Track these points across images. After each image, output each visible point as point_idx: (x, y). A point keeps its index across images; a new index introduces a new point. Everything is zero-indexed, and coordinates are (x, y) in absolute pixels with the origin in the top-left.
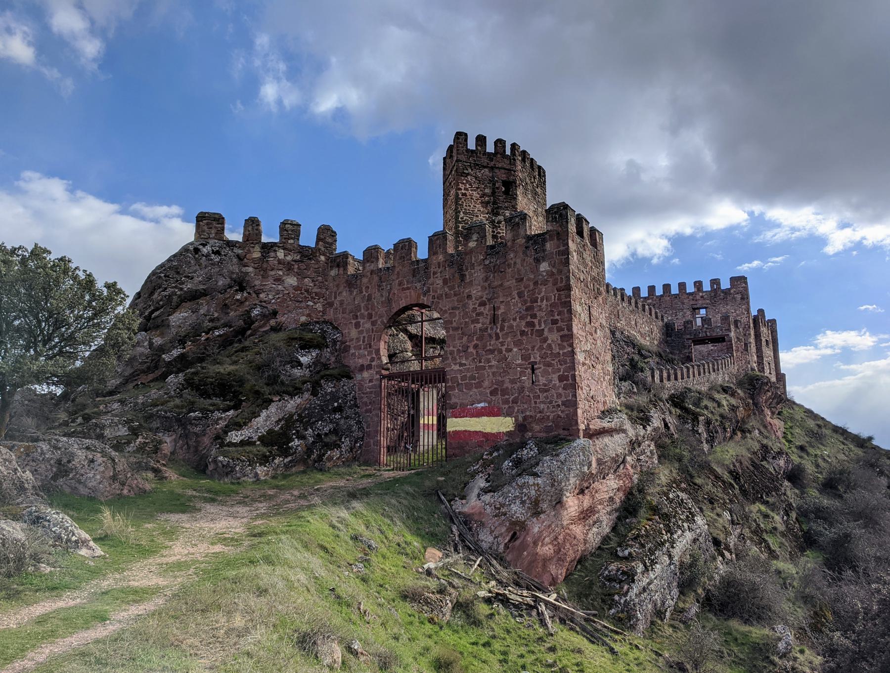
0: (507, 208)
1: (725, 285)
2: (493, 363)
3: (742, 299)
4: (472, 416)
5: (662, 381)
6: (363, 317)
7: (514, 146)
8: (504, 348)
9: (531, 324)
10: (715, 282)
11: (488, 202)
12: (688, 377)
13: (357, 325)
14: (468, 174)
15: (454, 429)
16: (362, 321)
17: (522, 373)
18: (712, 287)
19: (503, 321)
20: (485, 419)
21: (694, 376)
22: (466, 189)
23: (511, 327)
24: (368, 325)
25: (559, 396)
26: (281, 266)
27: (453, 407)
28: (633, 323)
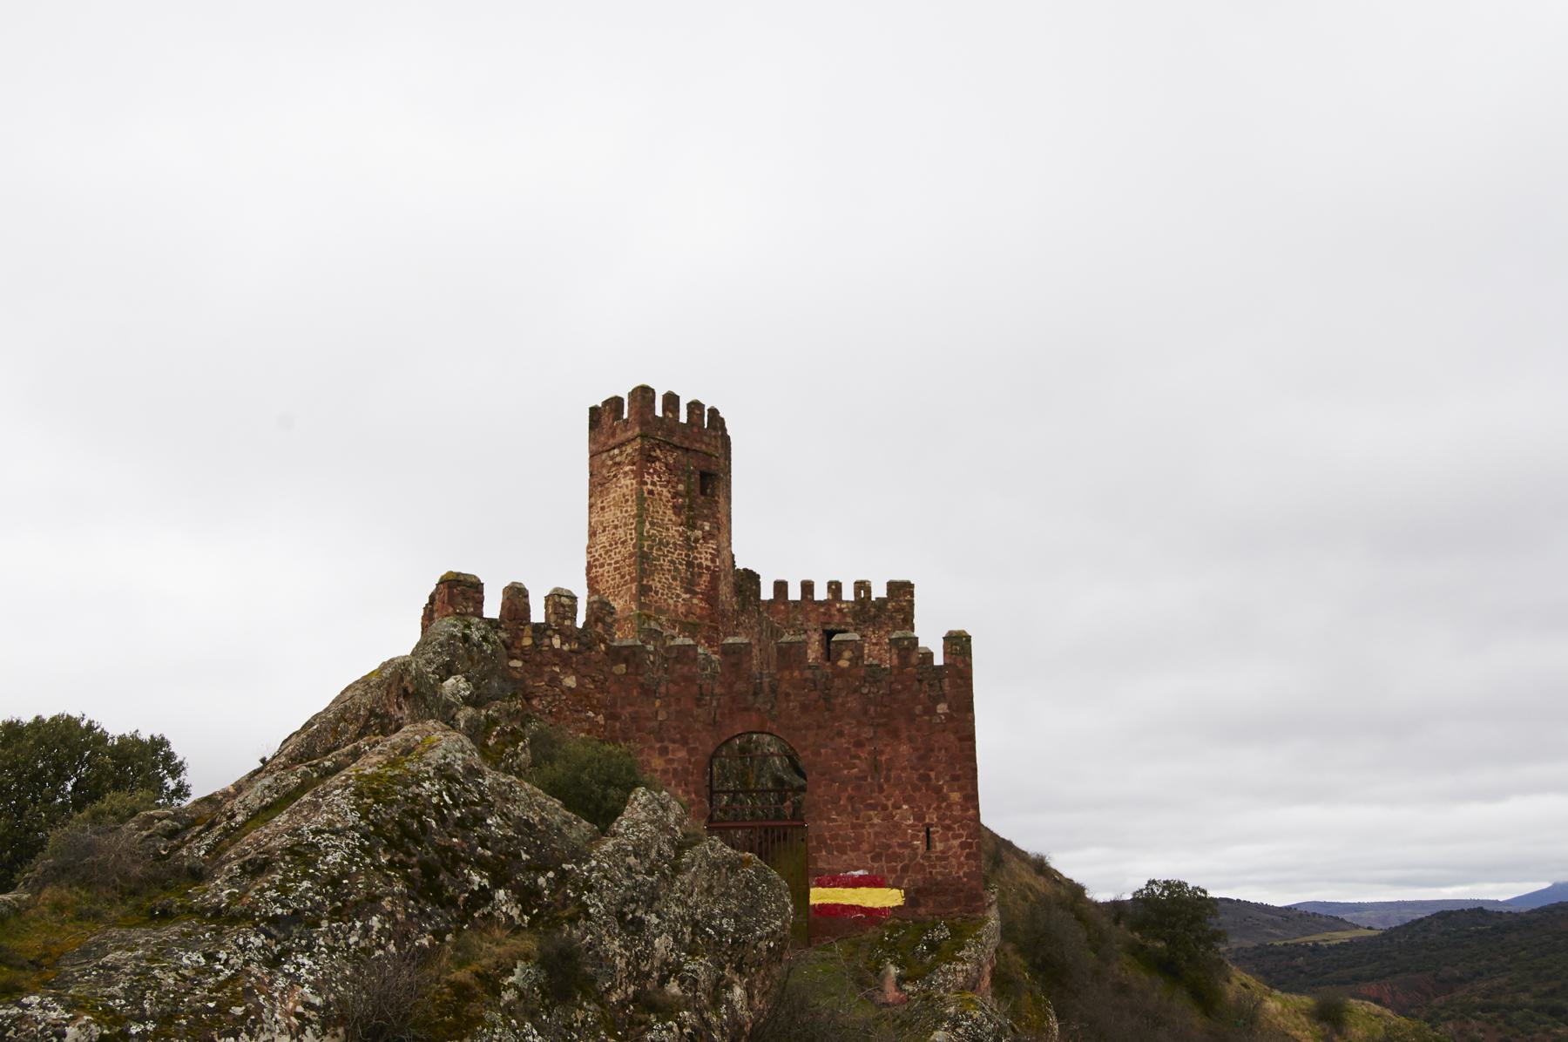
0: (706, 518)
1: (879, 591)
2: (876, 821)
4: (846, 885)
6: (674, 742)
8: (890, 804)
9: (925, 778)
10: (862, 586)
11: (682, 506)
13: (664, 751)
15: (818, 902)
16: (671, 746)
17: (914, 837)
18: (857, 594)
19: (889, 770)
20: (864, 890)
22: (653, 484)
23: (899, 777)
24: (682, 754)
25: (961, 865)
26: (556, 660)
27: (820, 873)
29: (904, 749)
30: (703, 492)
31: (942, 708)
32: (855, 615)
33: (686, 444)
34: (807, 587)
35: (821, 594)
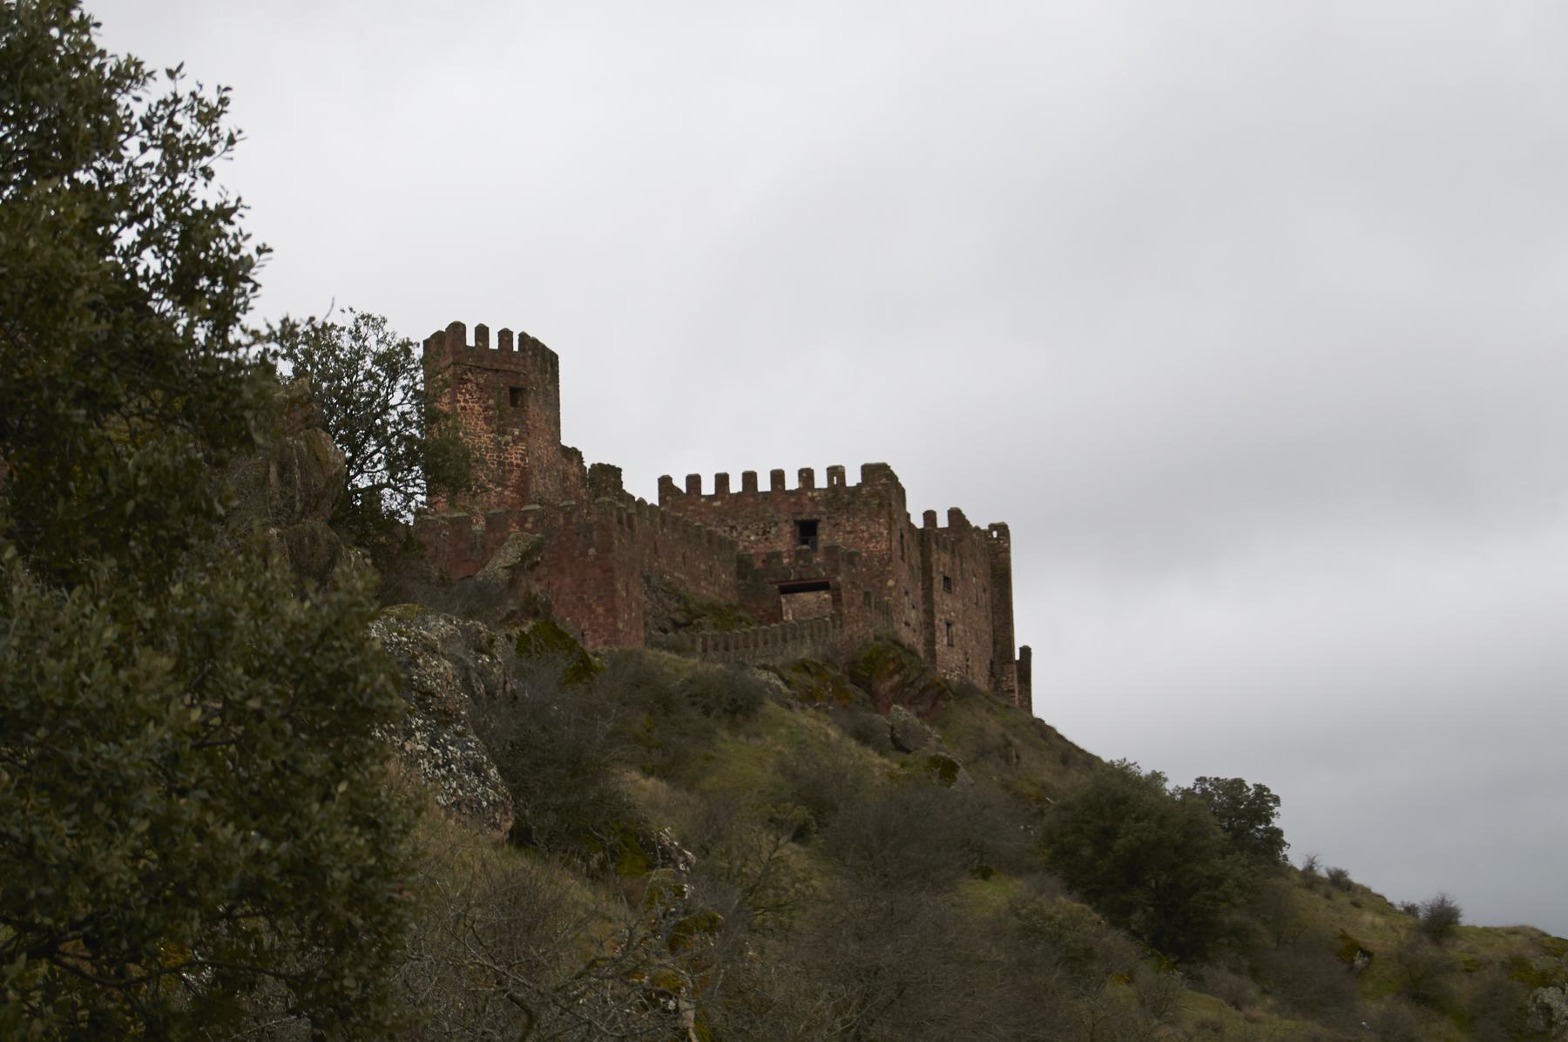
1: (853, 479)
3: (881, 505)
5: (705, 651)
7: (523, 336)
9: (581, 599)
10: (836, 472)
11: (492, 418)
12: (747, 647)
14: (469, 380)
18: (830, 480)
21: (756, 646)
22: (466, 401)
28: (679, 559)
29: (568, 580)
30: (514, 403)
31: (592, 551)
32: (828, 503)
33: (496, 366)
34: (778, 477)
35: (792, 483)
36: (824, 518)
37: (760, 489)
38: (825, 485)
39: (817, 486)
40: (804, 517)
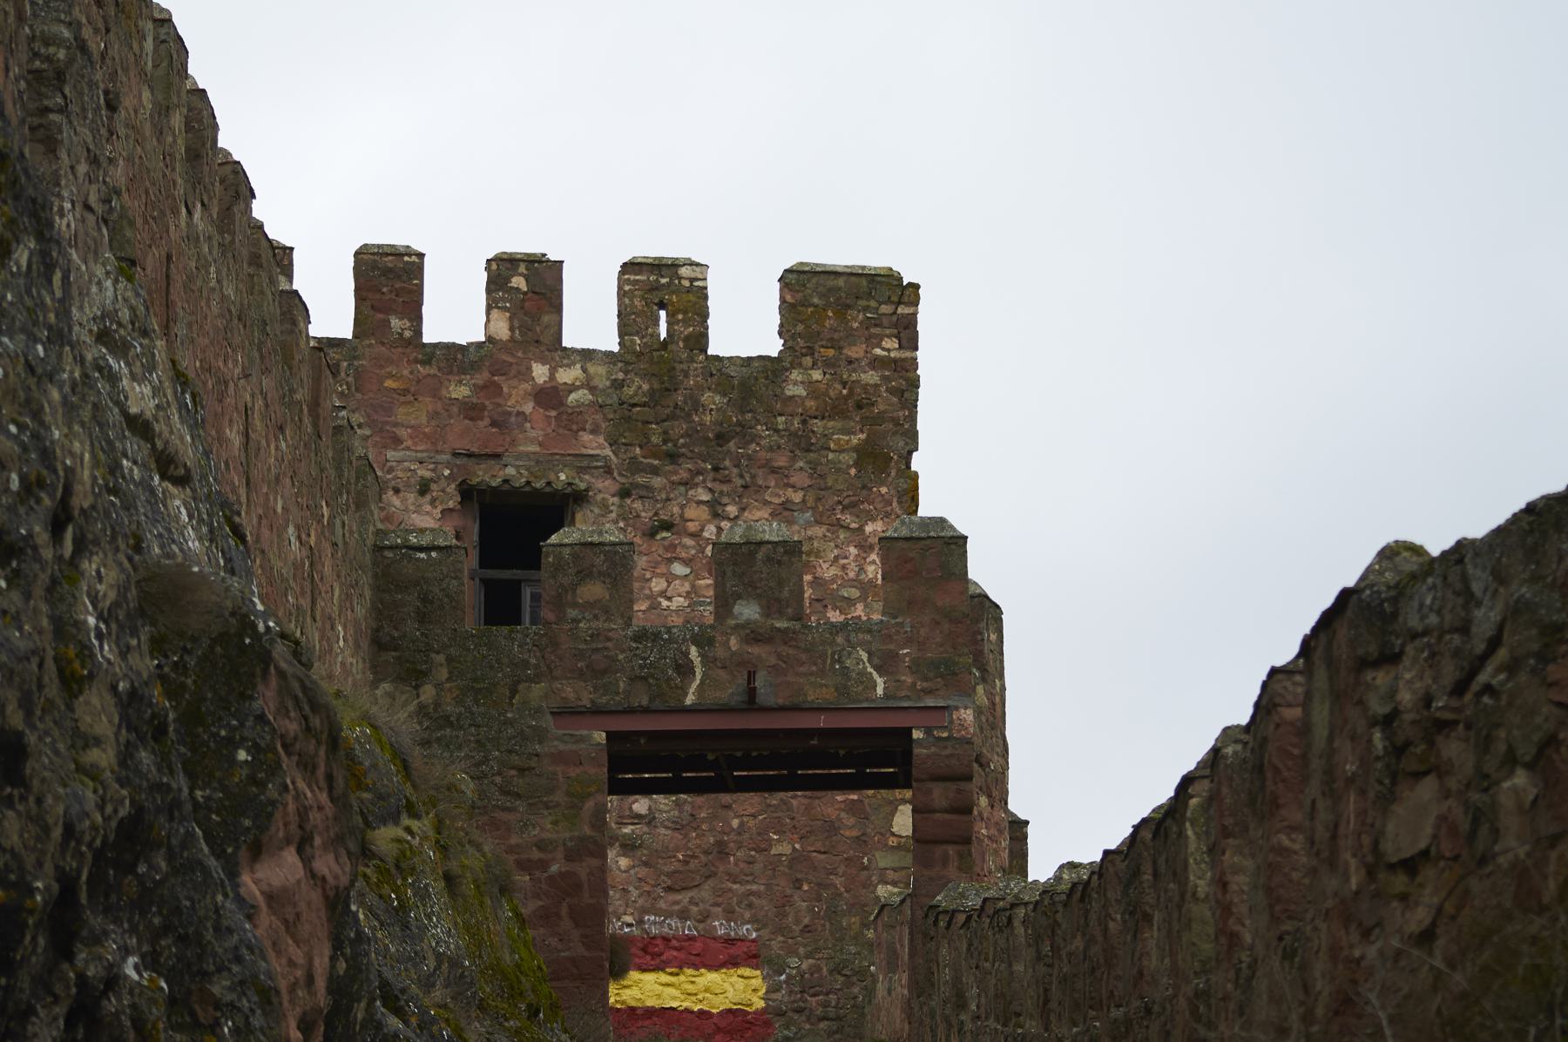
1: (744, 326)
10: (663, 292)
18: (628, 322)
32: (625, 420)
35: (455, 313)
36: (604, 488)
37: (319, 327)
38: (609, 341)
39: (572, 337)
40: (512, 473)
